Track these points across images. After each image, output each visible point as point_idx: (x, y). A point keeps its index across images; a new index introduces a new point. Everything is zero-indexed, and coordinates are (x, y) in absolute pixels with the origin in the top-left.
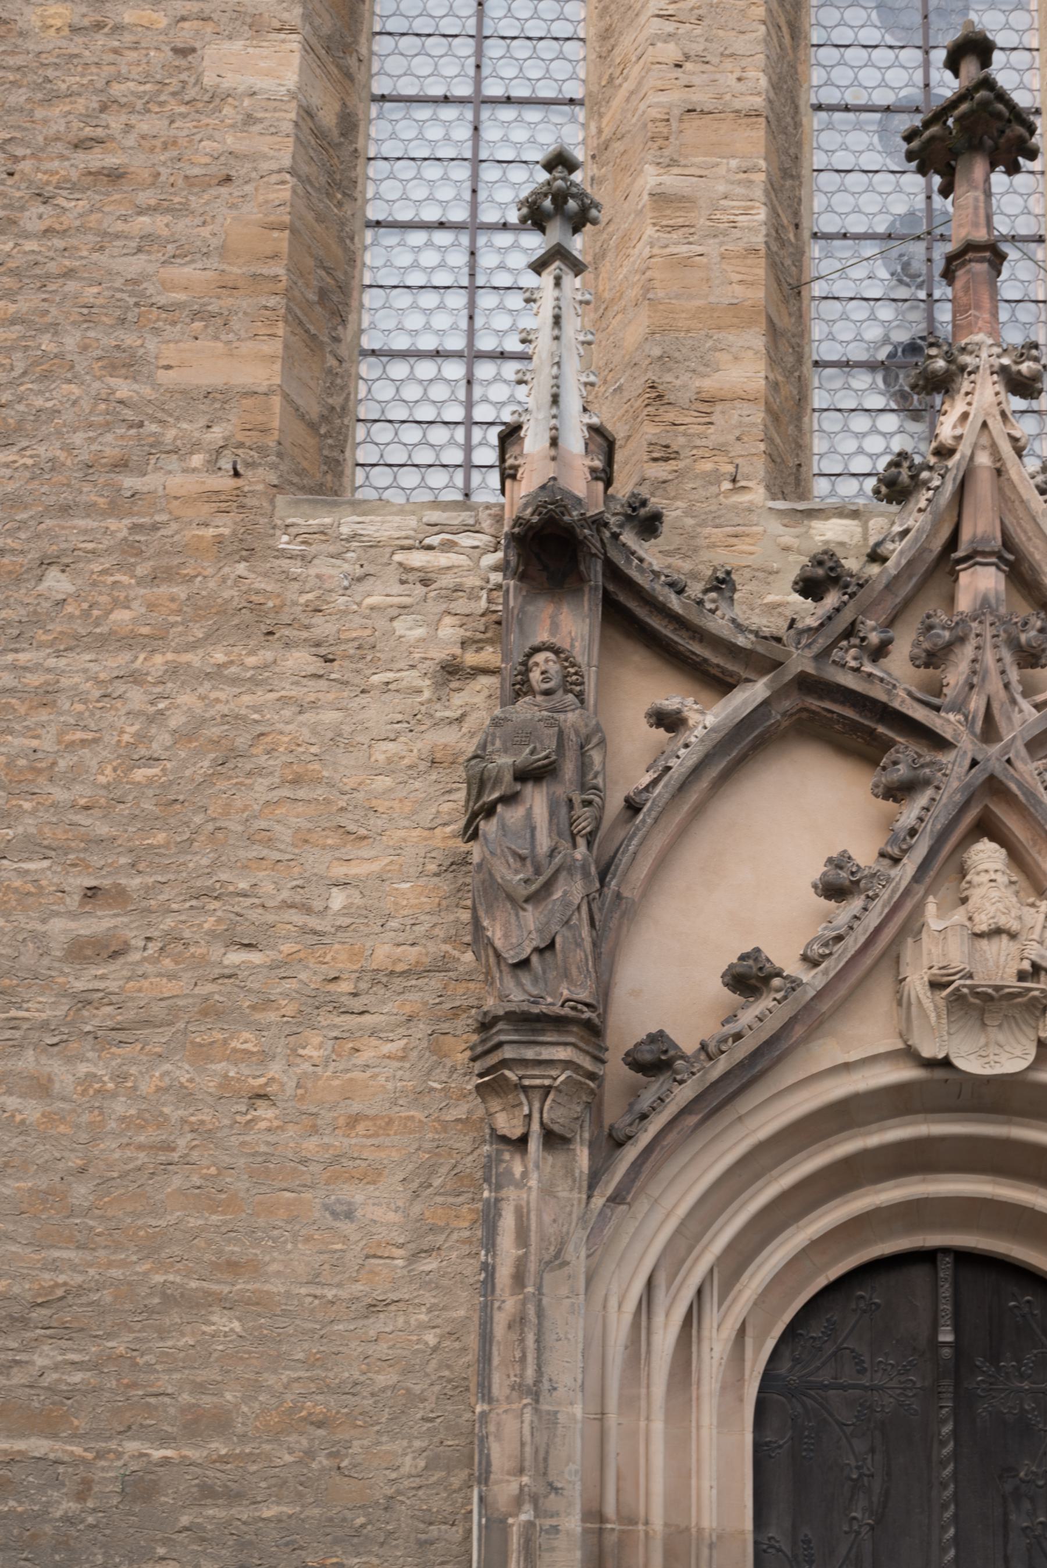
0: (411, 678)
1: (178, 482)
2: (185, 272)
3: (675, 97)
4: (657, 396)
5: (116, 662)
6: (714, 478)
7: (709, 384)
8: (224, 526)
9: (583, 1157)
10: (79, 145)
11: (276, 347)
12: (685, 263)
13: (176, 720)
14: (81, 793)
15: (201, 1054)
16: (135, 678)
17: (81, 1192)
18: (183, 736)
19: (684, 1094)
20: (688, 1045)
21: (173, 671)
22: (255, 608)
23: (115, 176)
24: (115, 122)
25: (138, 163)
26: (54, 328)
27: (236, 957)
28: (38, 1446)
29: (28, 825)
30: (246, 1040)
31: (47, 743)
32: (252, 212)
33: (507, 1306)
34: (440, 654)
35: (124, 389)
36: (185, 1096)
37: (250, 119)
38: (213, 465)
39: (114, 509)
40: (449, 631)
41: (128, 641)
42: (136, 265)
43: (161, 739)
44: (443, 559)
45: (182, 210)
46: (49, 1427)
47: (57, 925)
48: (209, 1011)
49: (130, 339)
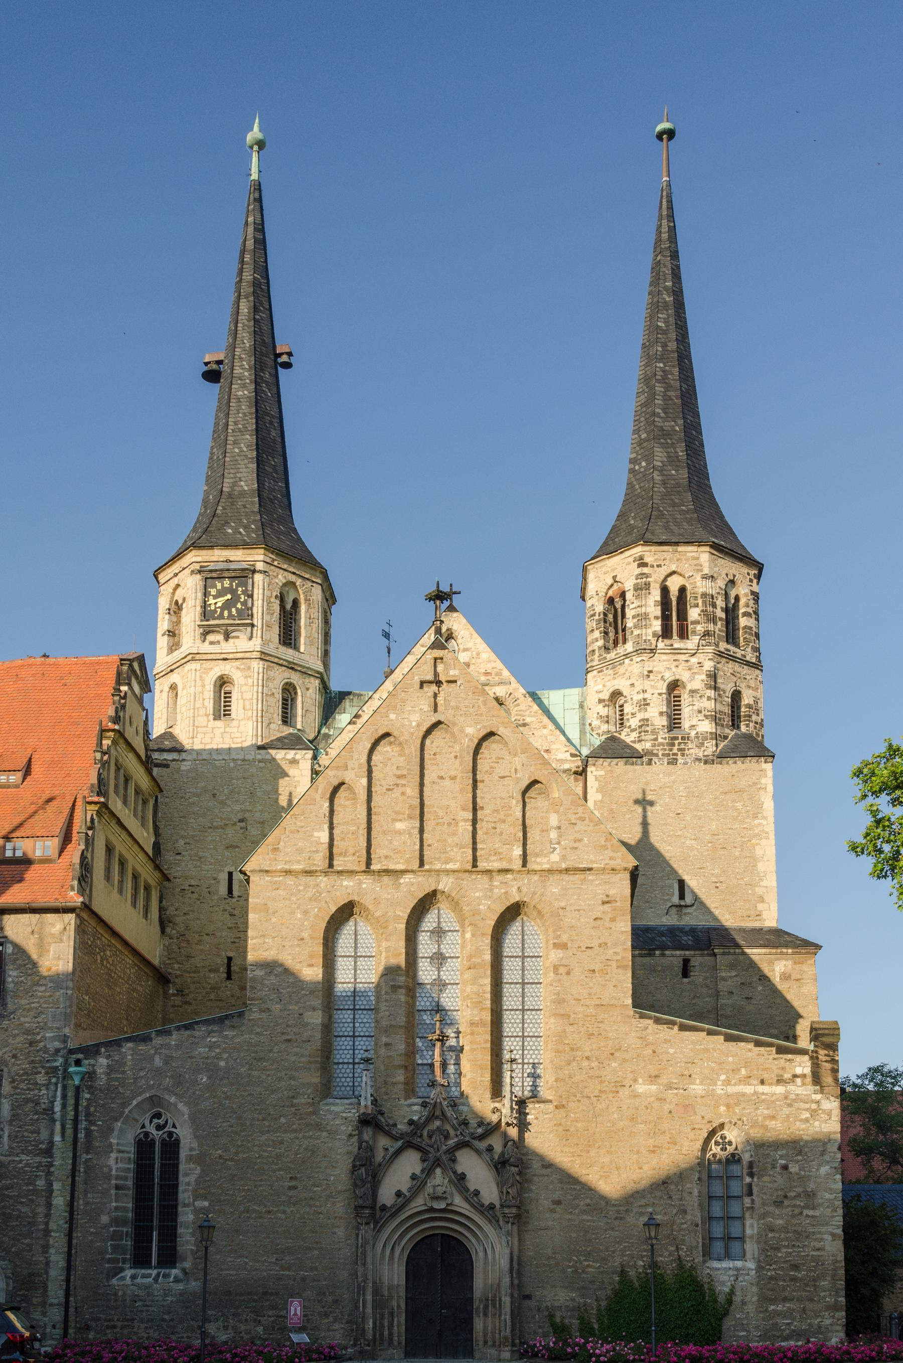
0: (344, 1137)
1: (303, 1100)
2: (303, 1059)
3: (388, 1023)
4: (386, 1083)
5: (293, 1135)
6: (395, 1099)
7: (394, 1080)
8: (311, 1109)
9: (372, 1226)
10: (283, 1034)
11: (319, 1074)
12: (389, 1057)
13: (304, 1146)
14: (288, 1159)
15: (310, 1206)
16: (297, 1138)
17: (292, 1230)
18: (306, 1149)
19: (388, 1215)
20: (389, 1205)
21: (304, 1137)
22: (317, 1125)
23: (289, 1040)
24: (289, 1029)
25: (294, 1037)
26: (280, 1071)
27: (315, 1189)
28: (287, 1273)
29: (280, 1166)
30: (318, 1204)
31: (283, 1150)
32: (314, 1047)
33: (360, 1250)
34: (349, 1133)
35: (293, 1083)
36: (308, 1213)
37: (313, 1029)
38: (308, 1097)
39: (292, 1106)
40: (350, 1128)
41: (295, 1131)
42: (294, 1058)
43: (302, 1150)
44: (349, 1115)
45: (301, 1047)
46: (289, 1269)
47: (286, 1184)
48: (311, 1198)
49: (294, 1073)
